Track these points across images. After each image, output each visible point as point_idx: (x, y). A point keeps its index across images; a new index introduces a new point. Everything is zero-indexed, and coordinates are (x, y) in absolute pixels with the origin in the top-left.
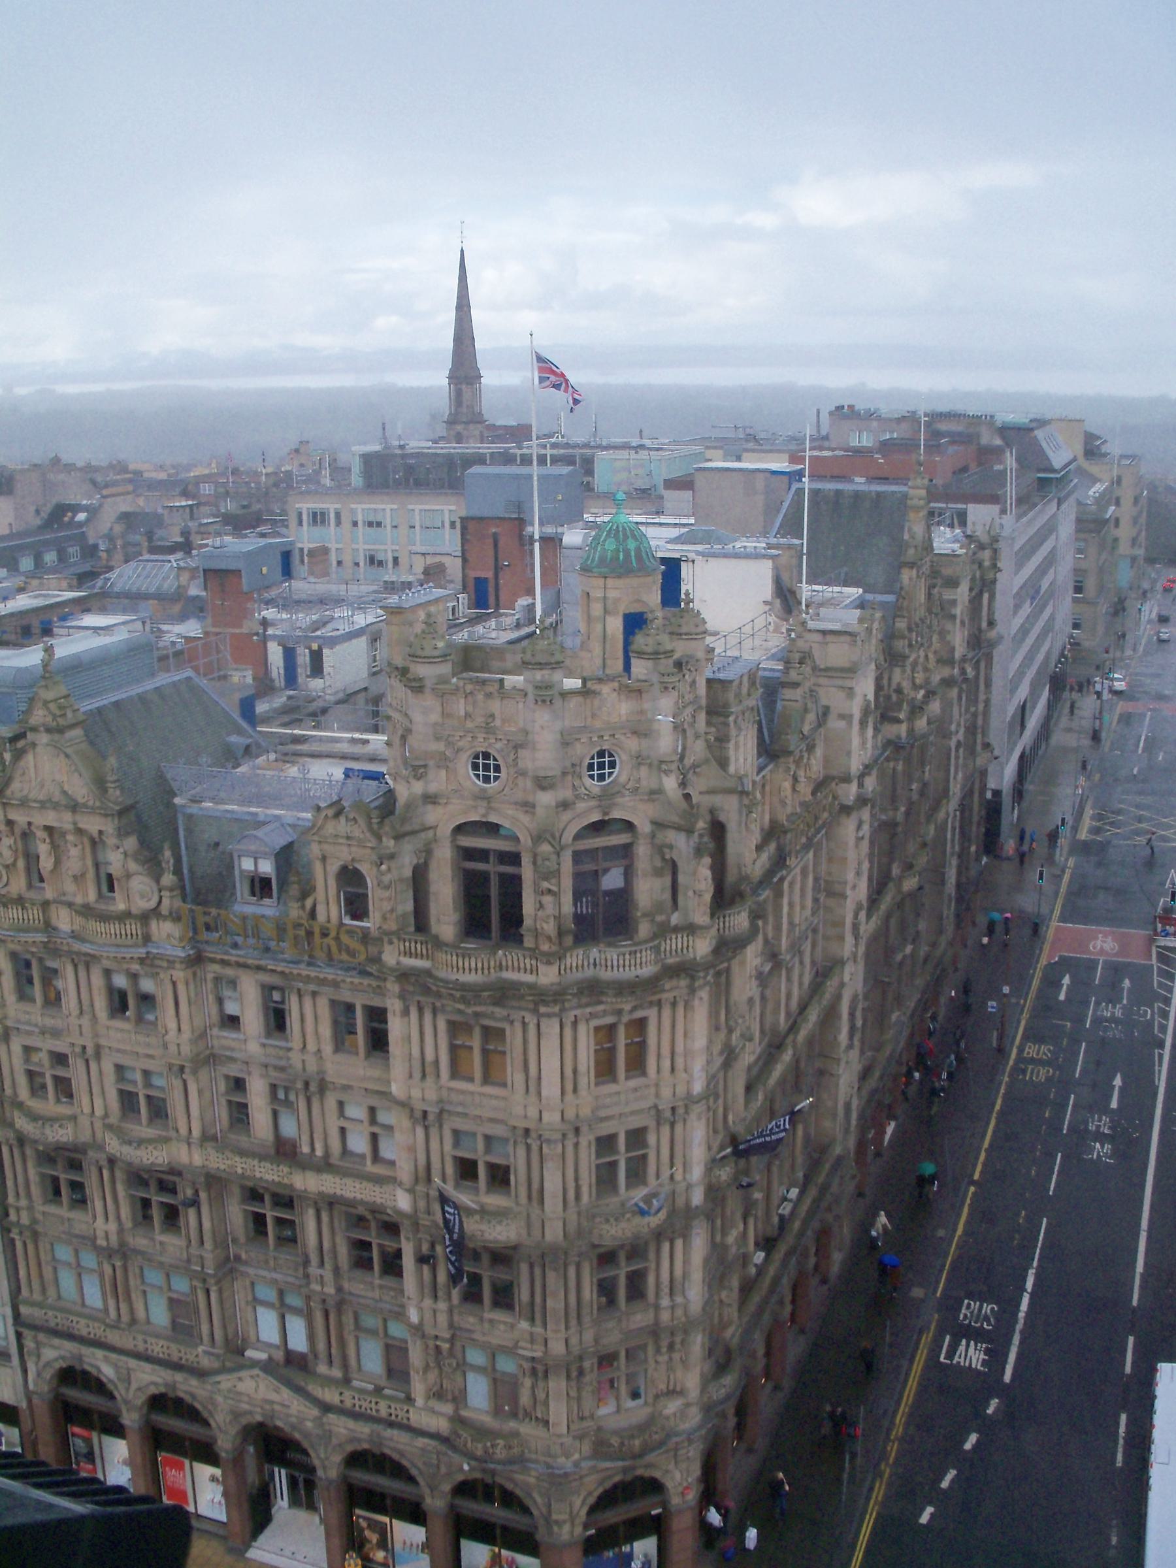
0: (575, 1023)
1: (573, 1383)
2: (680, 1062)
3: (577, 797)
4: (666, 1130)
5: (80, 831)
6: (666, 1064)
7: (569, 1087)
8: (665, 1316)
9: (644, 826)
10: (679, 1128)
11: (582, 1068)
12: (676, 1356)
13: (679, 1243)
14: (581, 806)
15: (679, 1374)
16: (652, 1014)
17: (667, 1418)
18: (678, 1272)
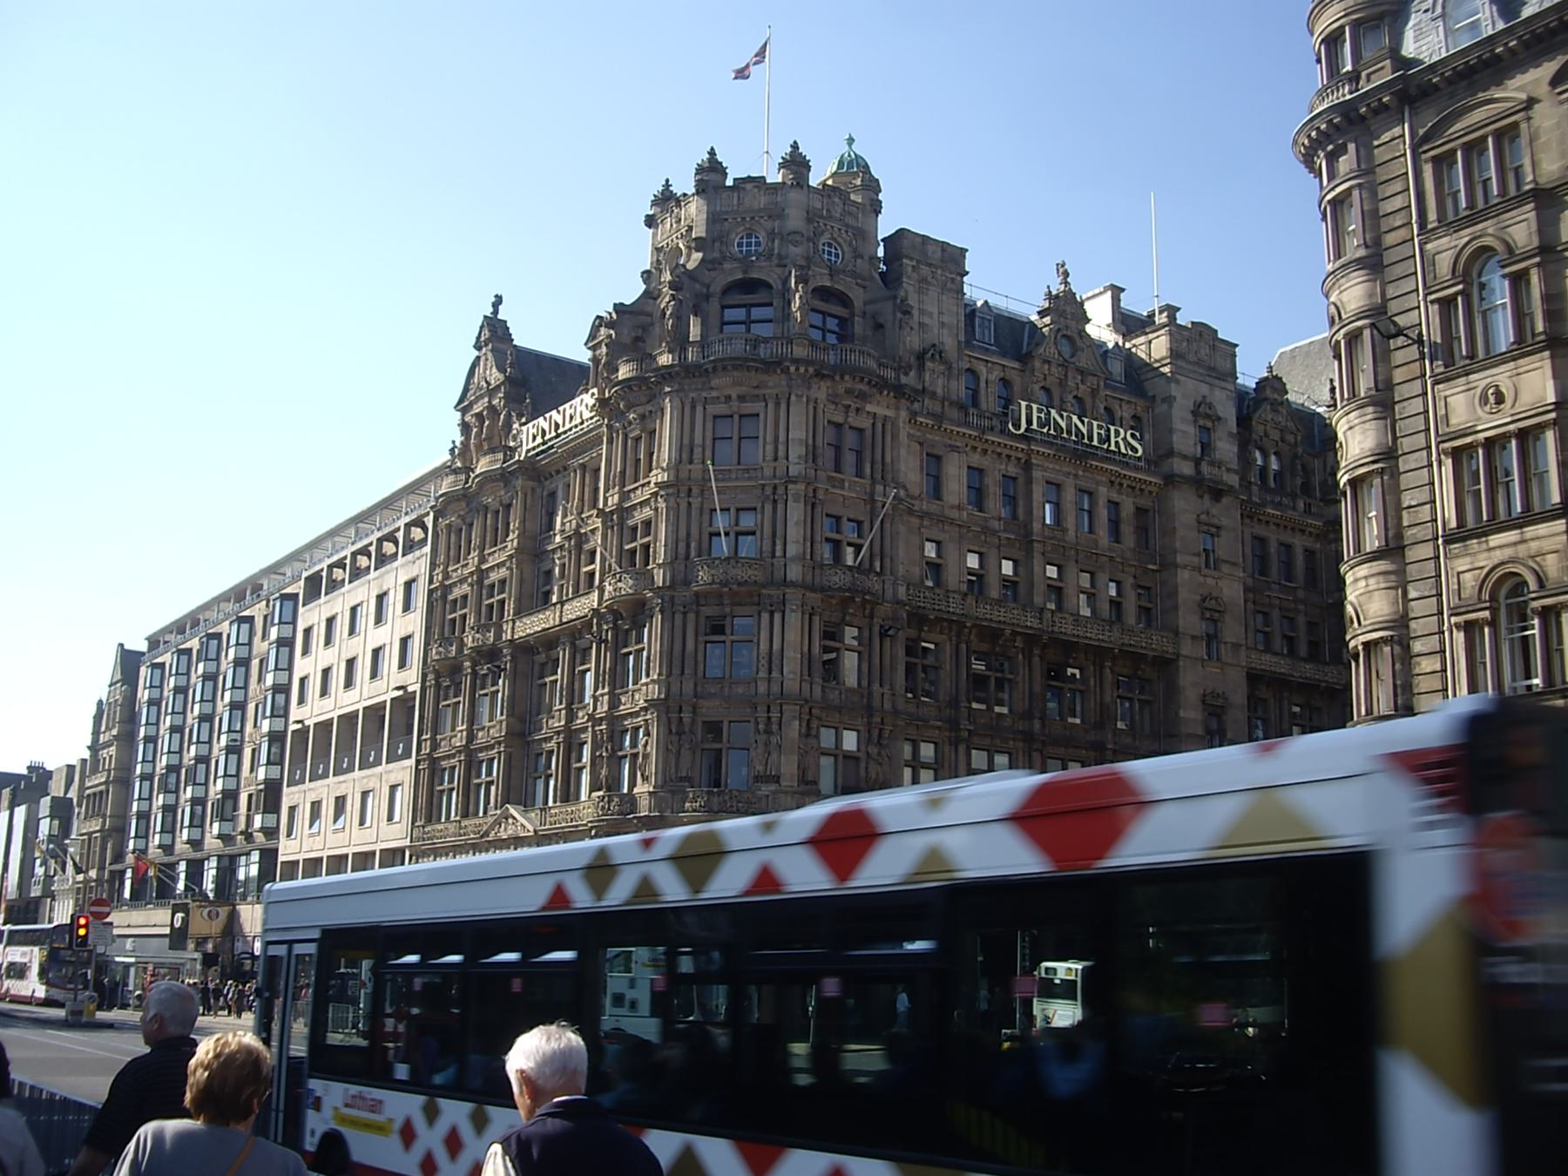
0: (693, 408)
1: (675, 738)
2: (781, 448)
3: (724, 258)
4: (768, 507)
5: (491, 408)
6: (769, 448)
7: (685, 456)
8: (762, 689)
9: (777, 285)
10: (780, 506)
11: (698, 440)
12: (774, 740)
13: (777, 617)
14: (727, 266)
15: (774, 756)
16: (758, 407)
17: (760, 799)
18: (776, 646)
